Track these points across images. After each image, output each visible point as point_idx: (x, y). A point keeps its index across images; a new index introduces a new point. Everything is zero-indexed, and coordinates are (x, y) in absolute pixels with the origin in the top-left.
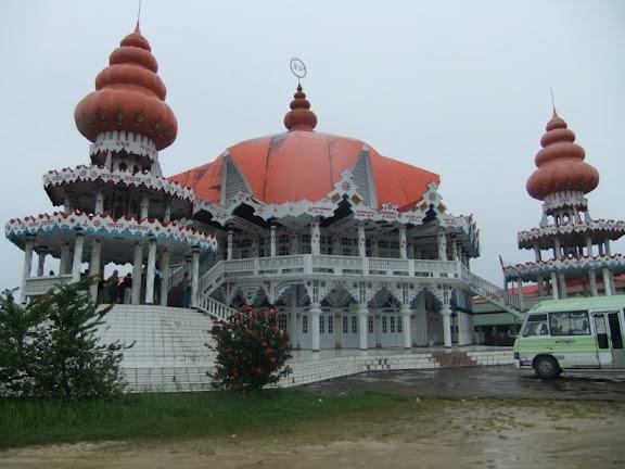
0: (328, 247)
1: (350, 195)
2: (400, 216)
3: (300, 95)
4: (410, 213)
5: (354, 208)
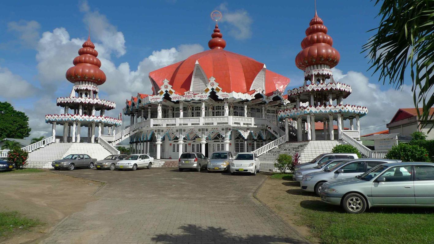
0: (165, 115)
1: (168, 90)
2: (194, 97)
4: (200, 95)
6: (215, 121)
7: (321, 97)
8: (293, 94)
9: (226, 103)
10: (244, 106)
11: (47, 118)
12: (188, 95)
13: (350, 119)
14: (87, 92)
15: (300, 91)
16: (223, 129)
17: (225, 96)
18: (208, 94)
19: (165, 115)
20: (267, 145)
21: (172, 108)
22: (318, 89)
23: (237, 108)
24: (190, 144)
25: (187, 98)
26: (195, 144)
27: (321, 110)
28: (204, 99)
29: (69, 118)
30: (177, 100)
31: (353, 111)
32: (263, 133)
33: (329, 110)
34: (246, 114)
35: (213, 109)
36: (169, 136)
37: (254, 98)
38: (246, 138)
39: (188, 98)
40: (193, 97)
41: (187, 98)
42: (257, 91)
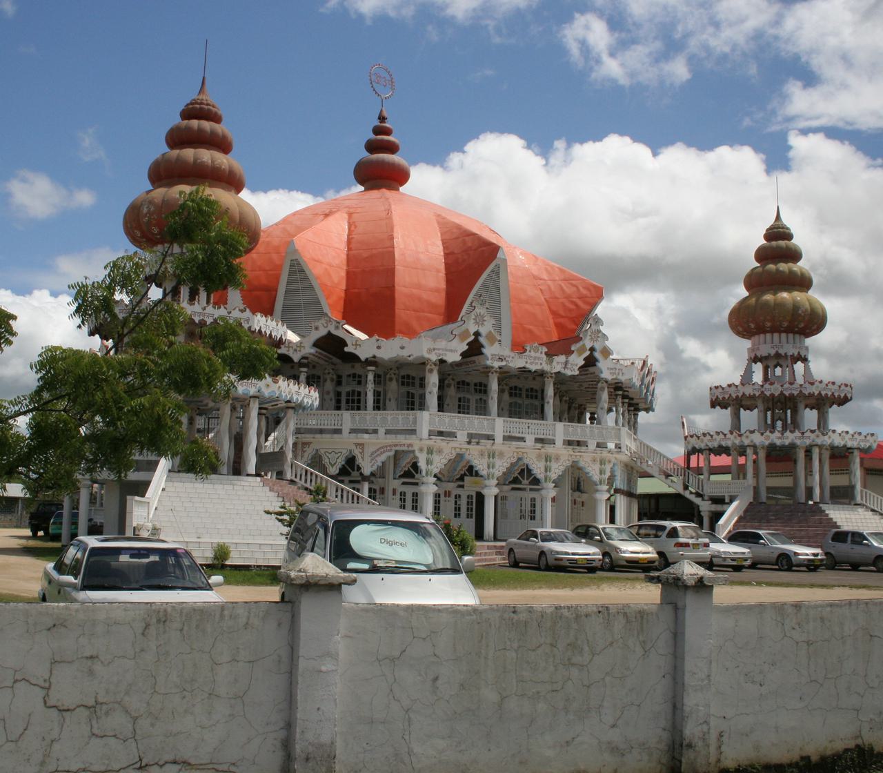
1: (484, 331)
5: (488, 351)
15: (789, 392)
17: (617, 371)
24: (447, 494)
26: (464, 493)
39: (531, 363)
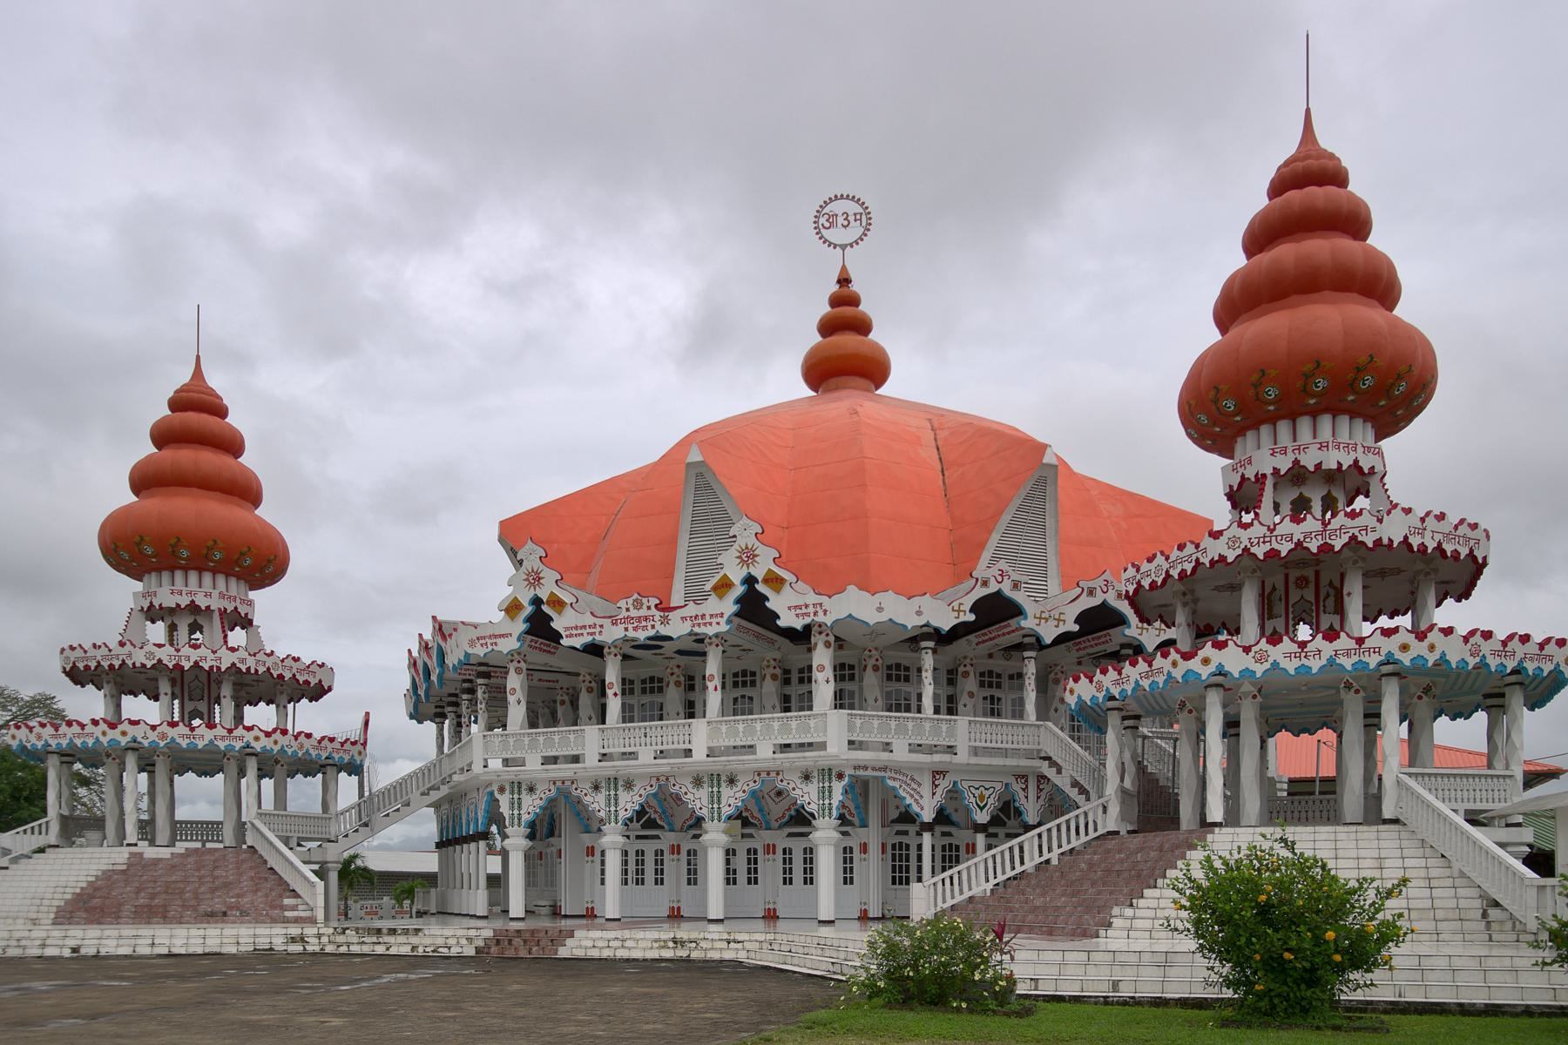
0: (543, 713)
3: (844, 298)
6: (765, 734)
7: (1309, 594)
8: (1146, 583)
9: (820, 646)
10: (920, 659)
11: (14, 737)
12: (634, 613)
13: (1487, 709)
14: (196, 615)
16: (807, 777)
17: (811, 610)
18: (728, 606)
19: (543, 713)
20: (1002, 853)
21: (594, 685)
22: (1275, 546)
23: (880, 670)
25: (630, 627)
27: (1275, 665)
28: (710, 631)
29: (102, 739)
30: (589, 639)
31: (1472, 661)
32: (1022, 794)
33: (1324, 662)
34: (928, 702)
35: (787, 682)
36: (578, 814)
37: (972, 617)
38: (928, 816)
39: (635, 629)
40: (658, 625)
41: (630, 627)
42: (985, 583)
